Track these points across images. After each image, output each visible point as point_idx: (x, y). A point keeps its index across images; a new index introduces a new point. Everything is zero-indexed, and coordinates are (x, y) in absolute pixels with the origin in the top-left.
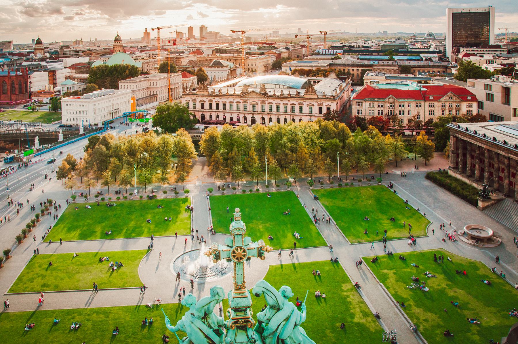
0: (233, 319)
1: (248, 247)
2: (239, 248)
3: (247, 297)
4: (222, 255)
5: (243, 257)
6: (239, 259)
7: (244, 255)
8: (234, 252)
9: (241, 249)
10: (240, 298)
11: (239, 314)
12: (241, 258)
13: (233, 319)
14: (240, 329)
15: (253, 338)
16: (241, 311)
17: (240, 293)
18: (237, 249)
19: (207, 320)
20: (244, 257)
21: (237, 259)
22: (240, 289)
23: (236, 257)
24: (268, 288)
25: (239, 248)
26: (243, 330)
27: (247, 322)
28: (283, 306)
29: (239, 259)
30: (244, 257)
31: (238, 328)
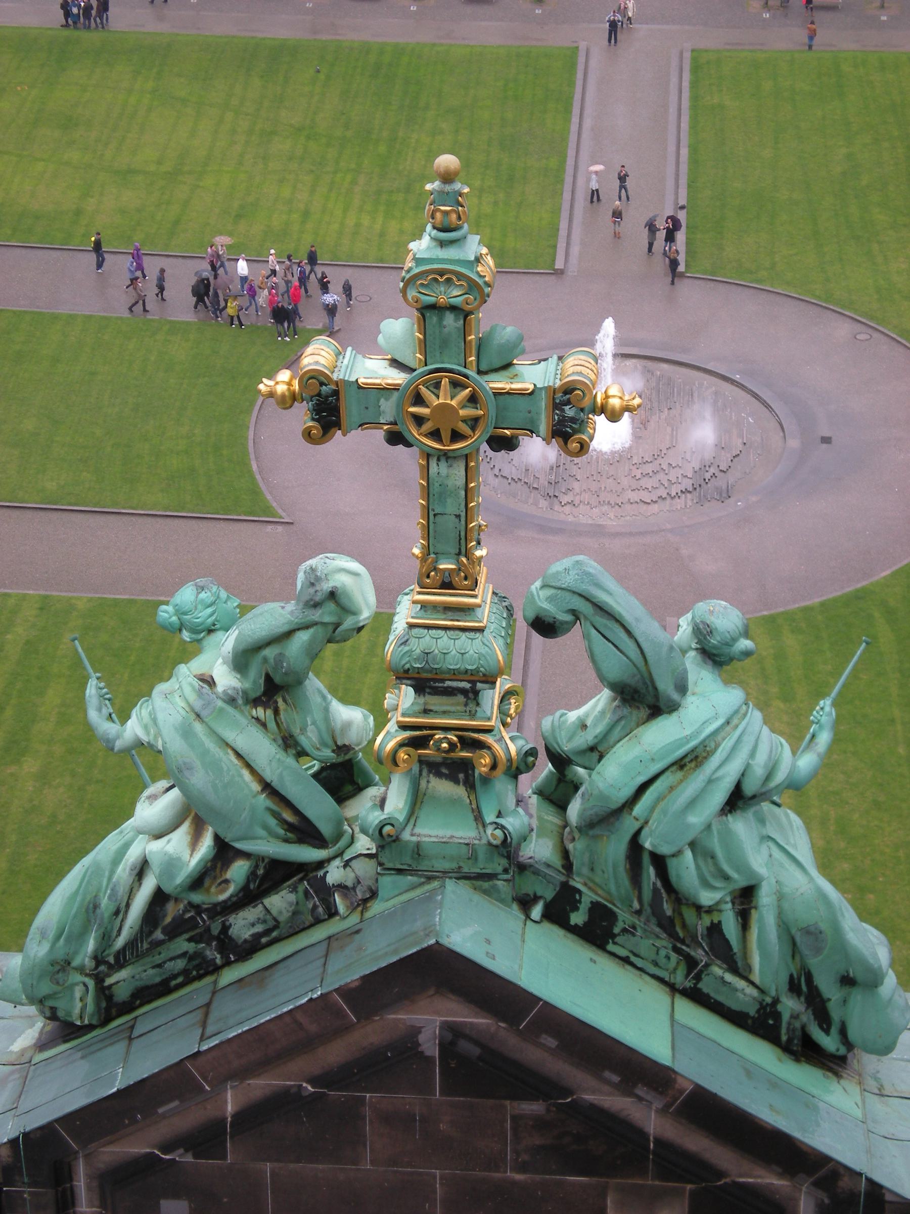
0: (404, 727)
1: (499, 382)
2: (445, 382)
3: (481, 630)
4: (350, 409)
5: (464, 428)
6: (446, 435)
7: (474, 422)
8: (419, 400)
9: (456, 385)
10: (446, 628)
11: (435, 702)
12: (456, 436)
13: (404, 727)
14: (439, 775)
15: (502, 828)
16: (449, 692)
17: (448, 609)
18: (437, 385)
19: (276, 712)
20: (473, 429)
21: (435, 435)
22: (447, 585)
23: (427, 427)
24: (602, 597)
25: (445, 382)
26: (456, 781)
27: (480, 745)
28: (675, 696)
29: (446, 435)
30: (473, 429)
31: (433, 767)
